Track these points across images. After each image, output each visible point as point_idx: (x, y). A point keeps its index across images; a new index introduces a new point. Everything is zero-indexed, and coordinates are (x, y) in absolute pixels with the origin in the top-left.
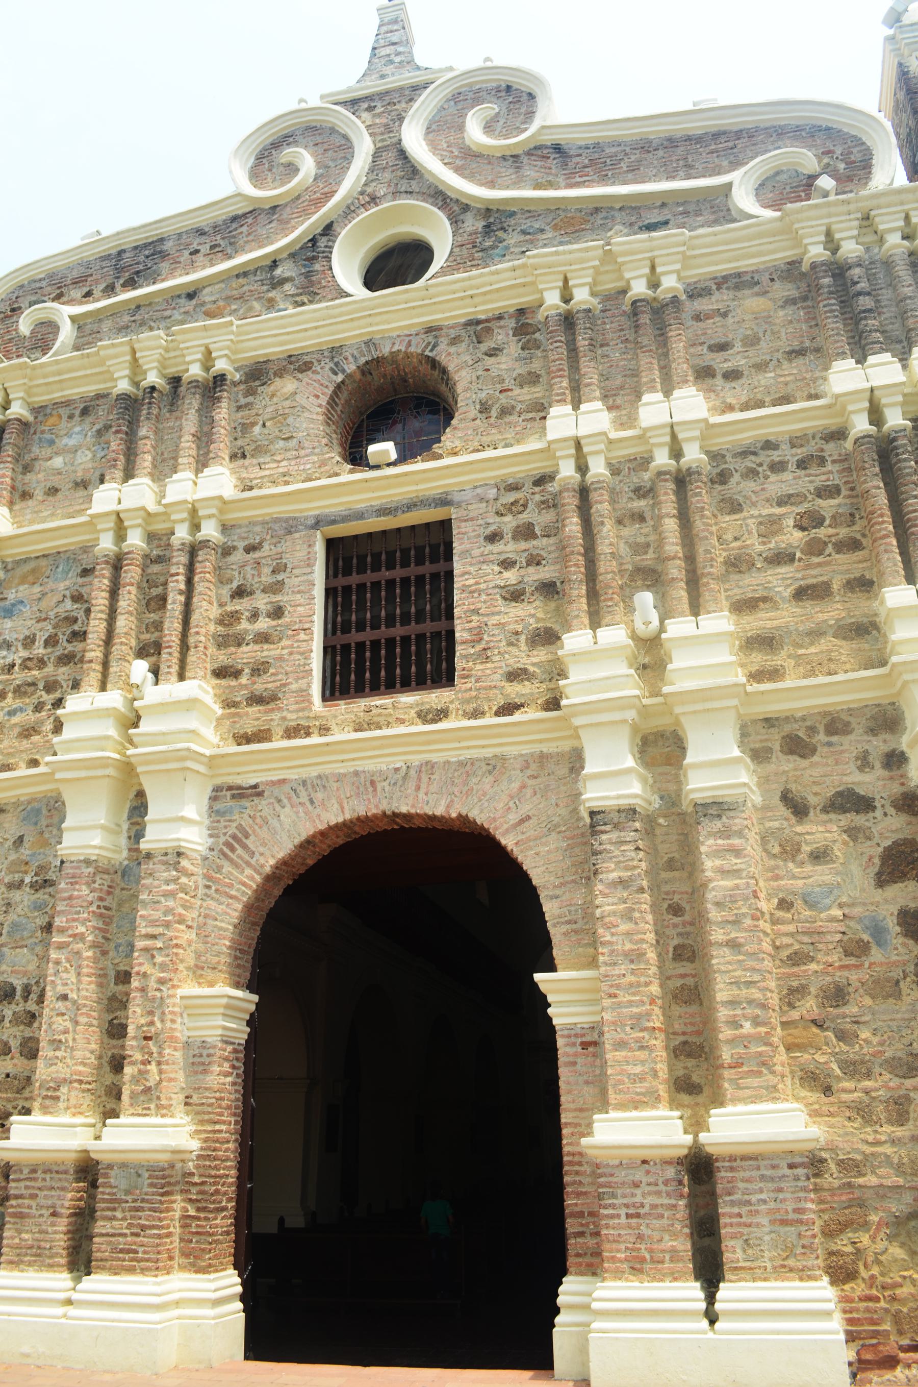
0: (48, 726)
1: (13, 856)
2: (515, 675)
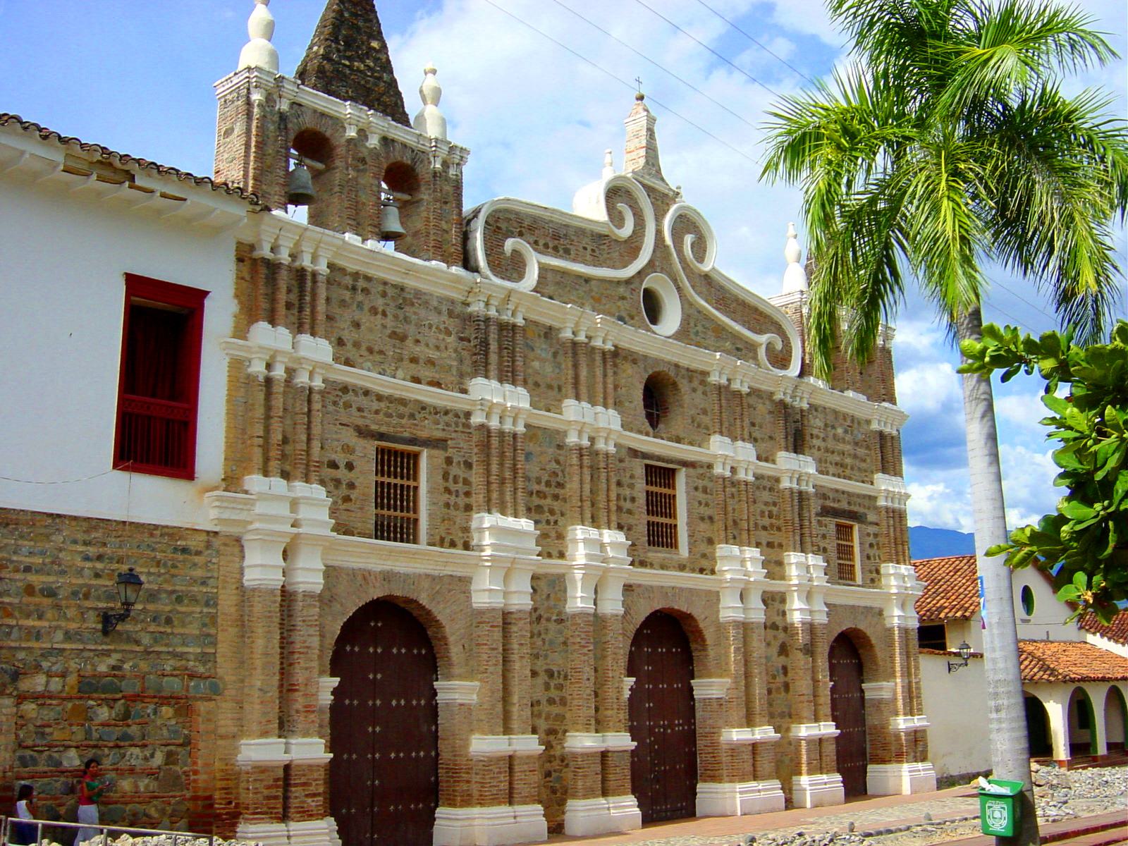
0: (553, 534)
1: (546, 604)
2: (704, 556)
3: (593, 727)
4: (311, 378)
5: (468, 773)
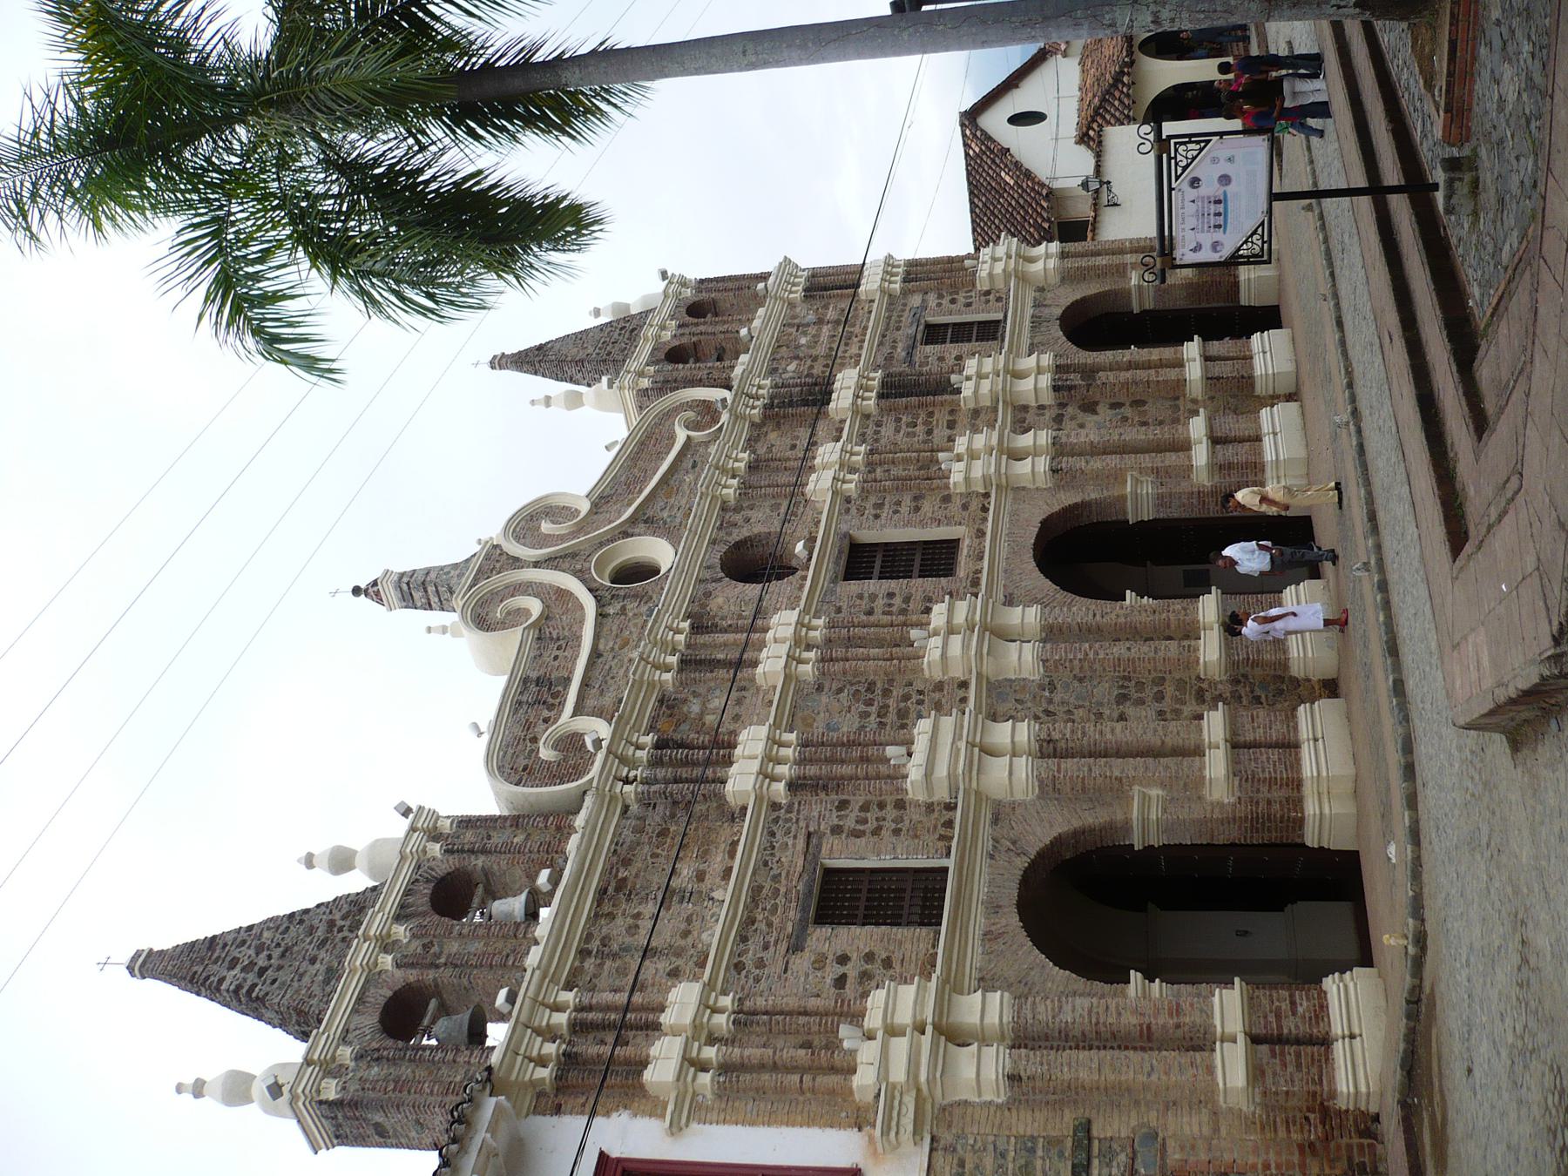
0: (937, 695)
1: (1029, 704)
3: (1193, 643)
4: (721, 1011)
5: (1257, 803)
